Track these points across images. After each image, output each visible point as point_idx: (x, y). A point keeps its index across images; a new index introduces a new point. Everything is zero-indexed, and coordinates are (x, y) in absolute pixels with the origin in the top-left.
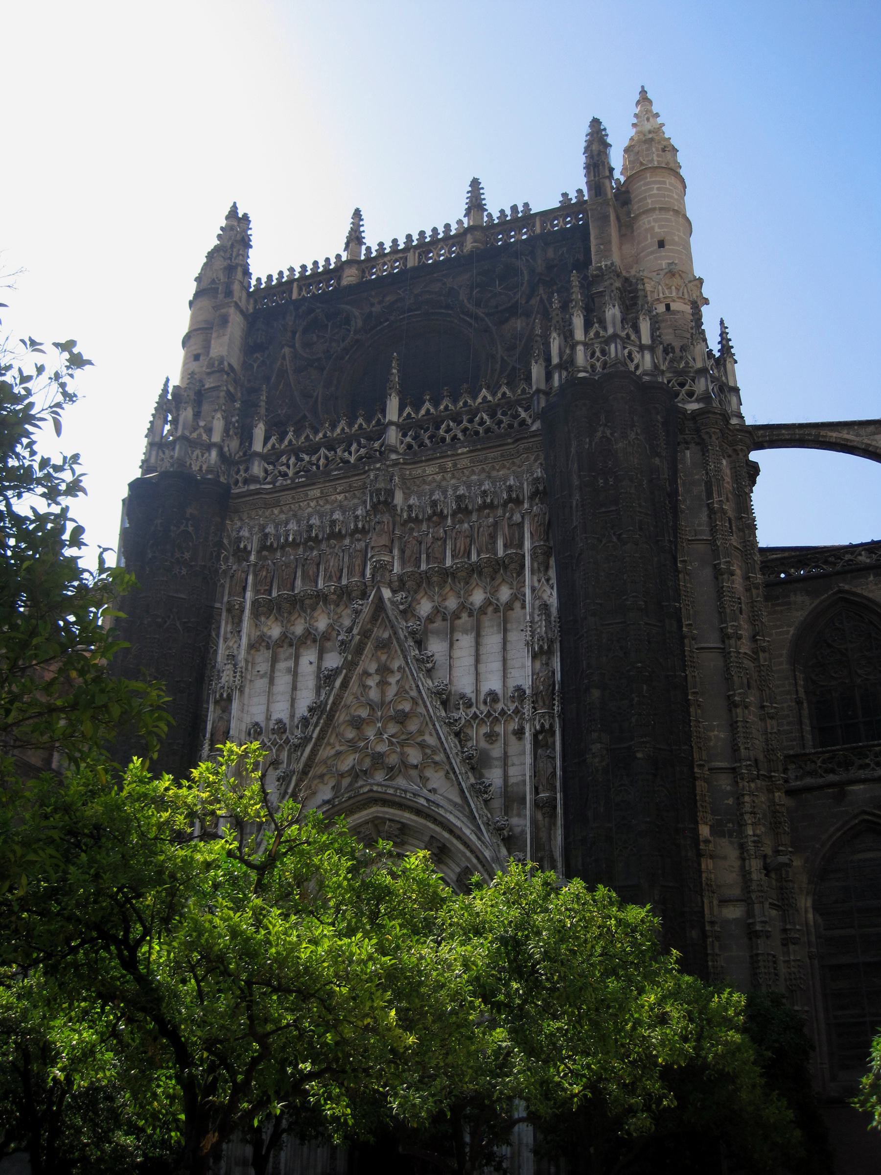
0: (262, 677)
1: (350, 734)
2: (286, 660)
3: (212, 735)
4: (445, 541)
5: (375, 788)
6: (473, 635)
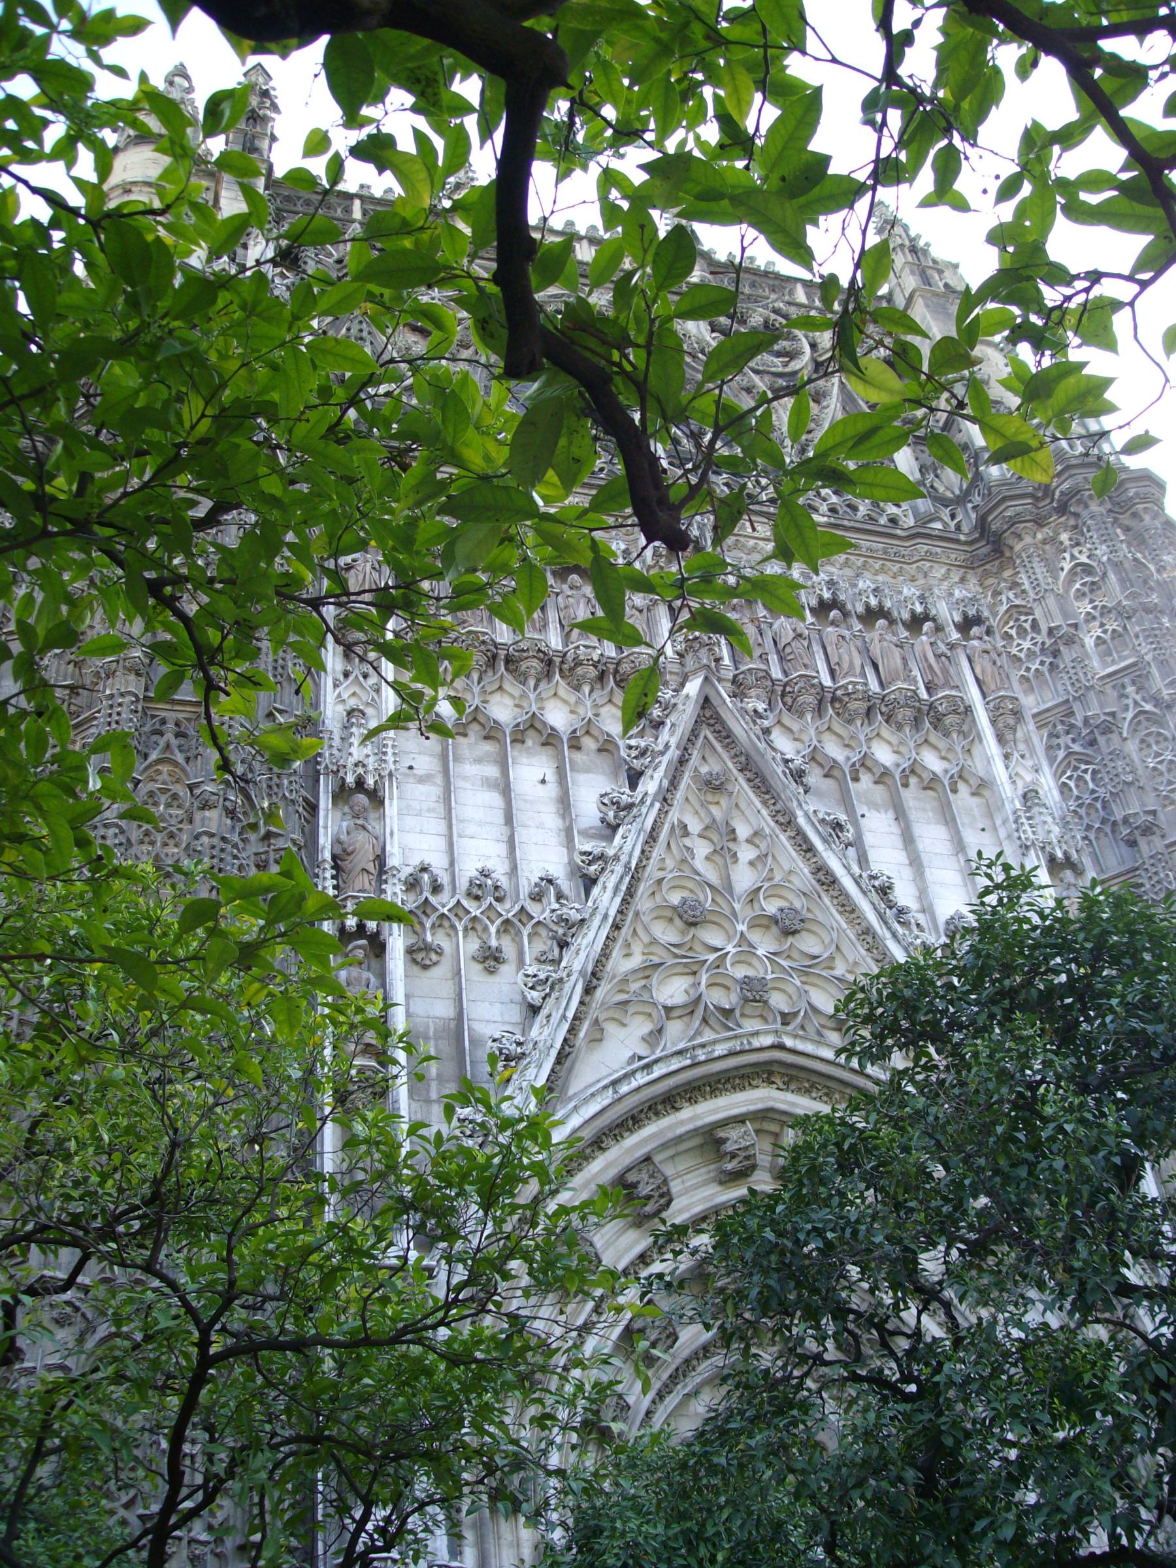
0: (422, 780)
1: (667, 934)
2: (478, 761)
3: (334, 857)
4: (810, 644)
5: (789, 1042)
6: (891, 815)
